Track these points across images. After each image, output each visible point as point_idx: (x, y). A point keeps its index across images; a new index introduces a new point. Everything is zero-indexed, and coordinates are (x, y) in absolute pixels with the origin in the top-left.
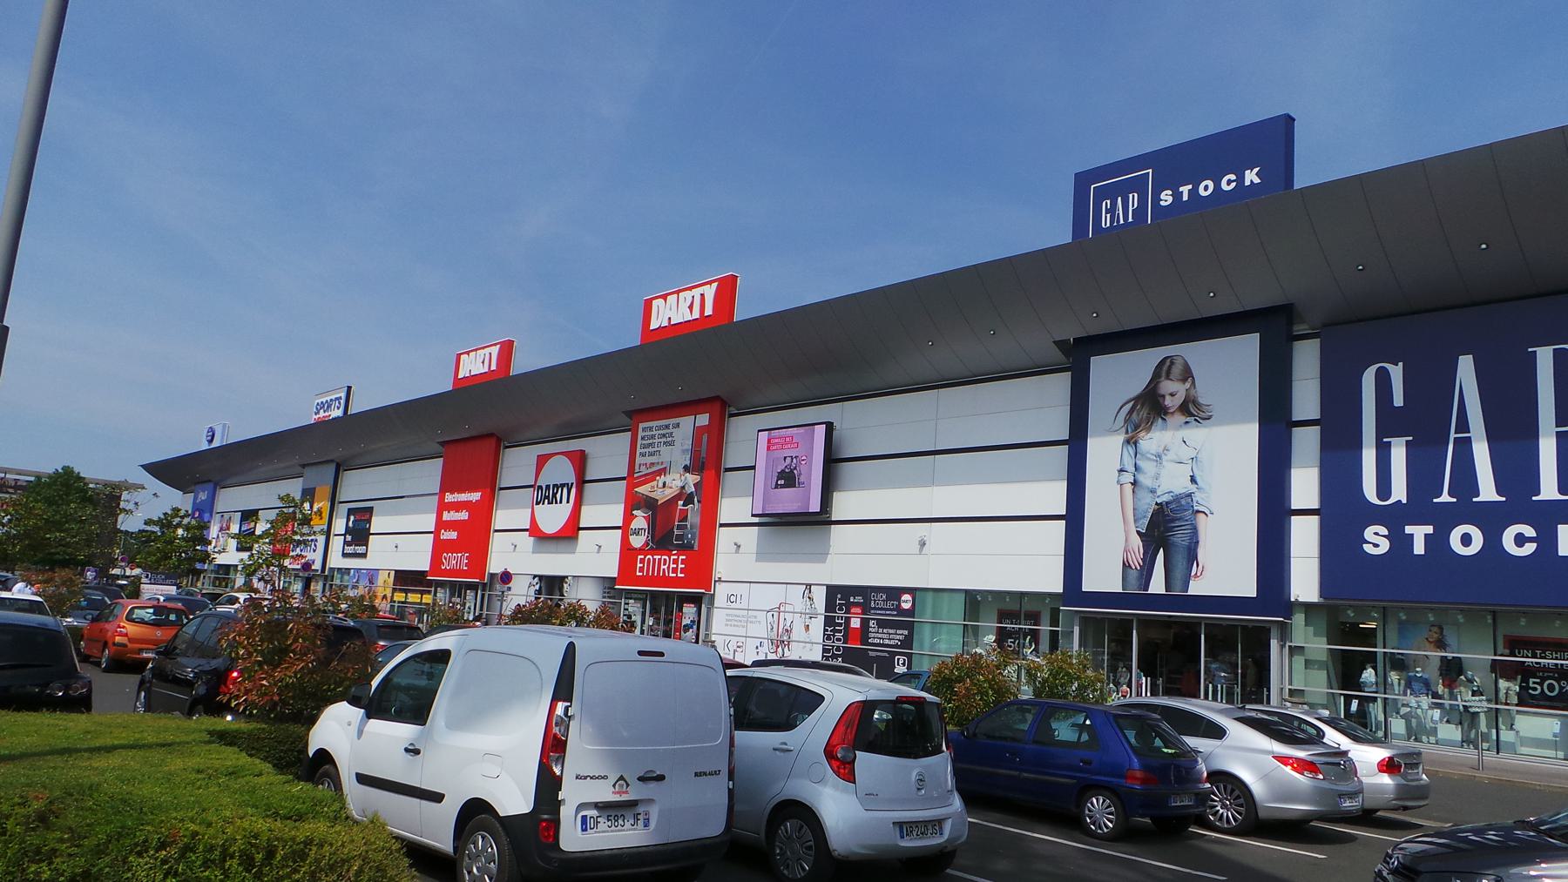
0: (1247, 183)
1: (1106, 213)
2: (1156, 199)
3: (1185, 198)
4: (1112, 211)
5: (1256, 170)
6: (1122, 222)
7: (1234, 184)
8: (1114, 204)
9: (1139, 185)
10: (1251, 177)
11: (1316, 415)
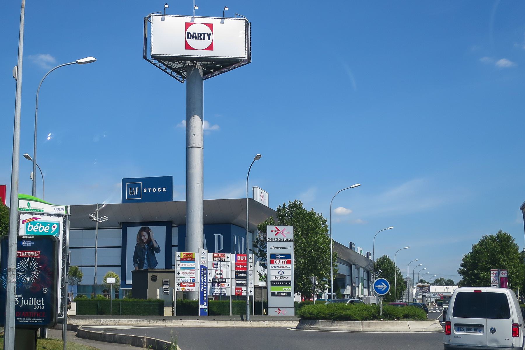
0: (163, 191)
1: (131, 191)
2: (143, 190)
3: (150, 191)
4: (132, 191)
5: (165, 188)
6: (134, 194)
7: (160, 191)
8: (132, 189)
9: (139, 186)
10: (164, 190)
11: (177, 244)
